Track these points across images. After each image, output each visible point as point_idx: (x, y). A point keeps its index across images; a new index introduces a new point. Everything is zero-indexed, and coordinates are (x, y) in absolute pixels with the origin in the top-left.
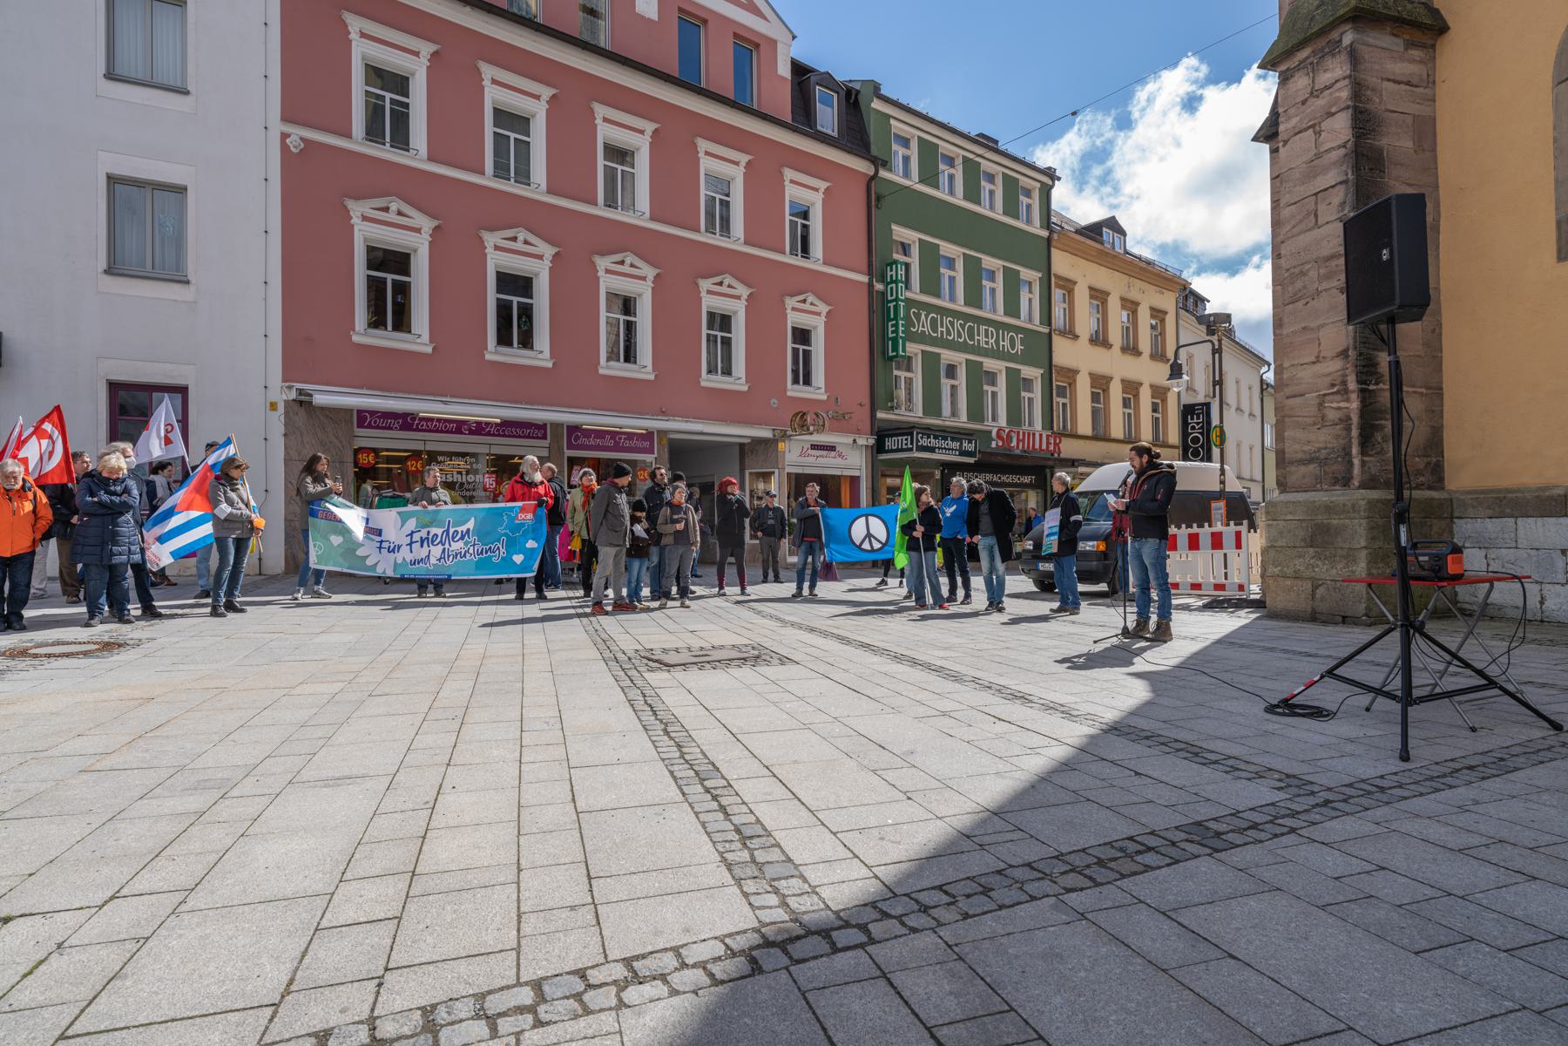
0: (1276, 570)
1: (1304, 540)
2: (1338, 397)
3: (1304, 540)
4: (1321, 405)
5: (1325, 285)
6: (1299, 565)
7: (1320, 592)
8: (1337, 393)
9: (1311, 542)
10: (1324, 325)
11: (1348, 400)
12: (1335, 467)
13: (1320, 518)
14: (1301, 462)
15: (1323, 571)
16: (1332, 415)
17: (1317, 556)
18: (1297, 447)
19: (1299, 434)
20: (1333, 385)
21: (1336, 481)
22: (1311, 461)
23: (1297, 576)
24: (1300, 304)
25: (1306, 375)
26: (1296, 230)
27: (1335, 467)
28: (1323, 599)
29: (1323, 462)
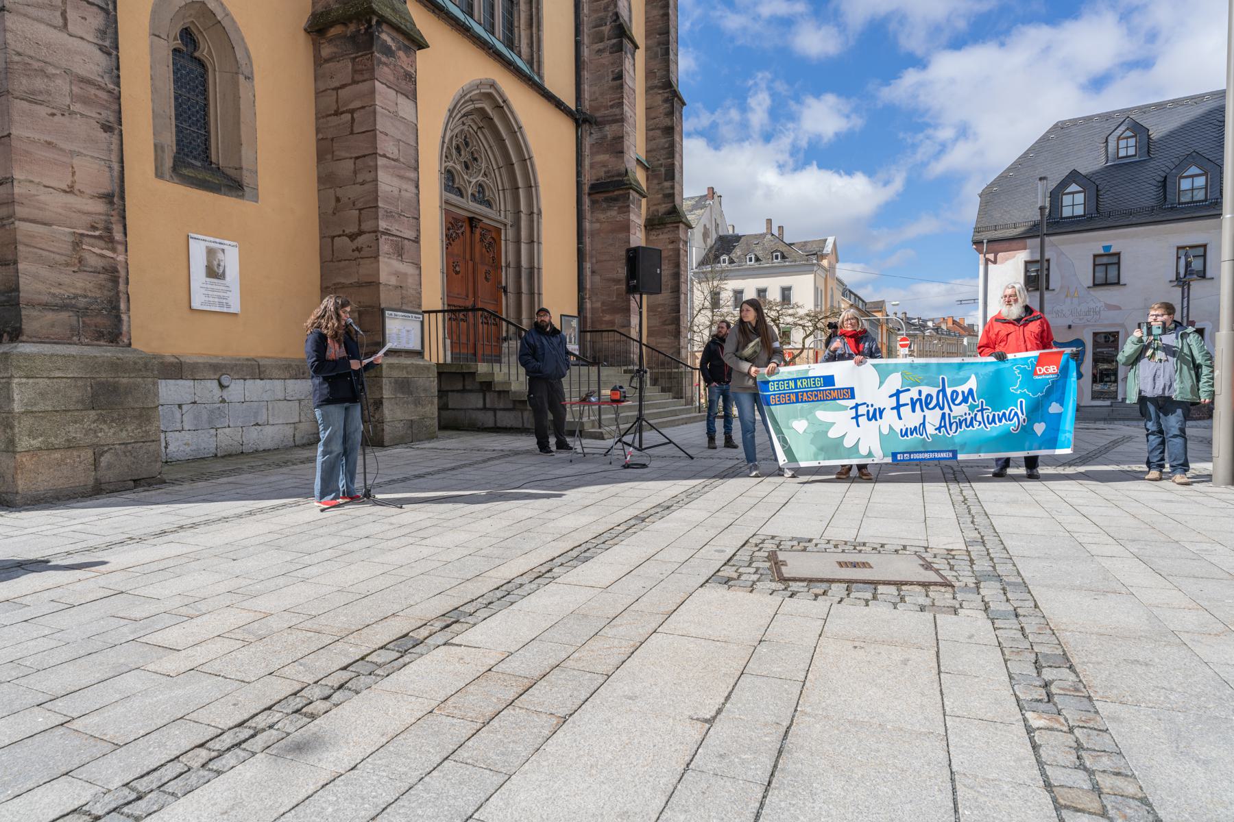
0: (36, 443)
1: (83, 402)
2: (102, 243)
3: (83, 402)
4: (77, 245)
5: (77, 107)
6: (75, 431)
7: (104, 460)
8: (100, 237)
9: (93, 402)
10: (79, 154)
11: (114, 250)
12: (98, 320)
13: (104, 376)
14: (46, 306)
15: (108, 434)
16: (93, 261)
17: (101, 419)
18: (41, 287)
19: (44, 272)
20: (94, 228)
21: (100, 336)
22: (63, 307)
23: (70, 446)
24: (43, 111)
25: (55, 203)
26: (30, 10)
27: (98, 320)
28: (110, 466)
29: (82, 312)
